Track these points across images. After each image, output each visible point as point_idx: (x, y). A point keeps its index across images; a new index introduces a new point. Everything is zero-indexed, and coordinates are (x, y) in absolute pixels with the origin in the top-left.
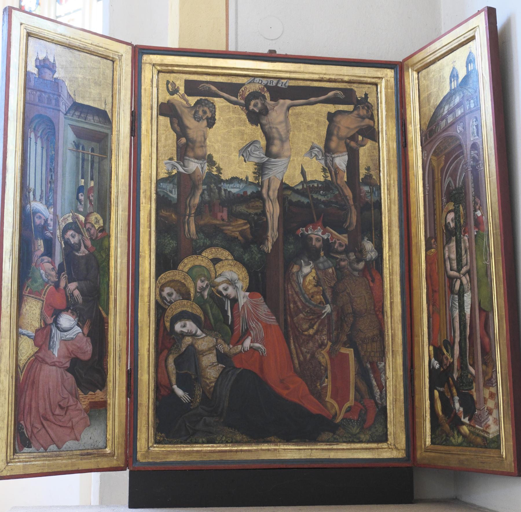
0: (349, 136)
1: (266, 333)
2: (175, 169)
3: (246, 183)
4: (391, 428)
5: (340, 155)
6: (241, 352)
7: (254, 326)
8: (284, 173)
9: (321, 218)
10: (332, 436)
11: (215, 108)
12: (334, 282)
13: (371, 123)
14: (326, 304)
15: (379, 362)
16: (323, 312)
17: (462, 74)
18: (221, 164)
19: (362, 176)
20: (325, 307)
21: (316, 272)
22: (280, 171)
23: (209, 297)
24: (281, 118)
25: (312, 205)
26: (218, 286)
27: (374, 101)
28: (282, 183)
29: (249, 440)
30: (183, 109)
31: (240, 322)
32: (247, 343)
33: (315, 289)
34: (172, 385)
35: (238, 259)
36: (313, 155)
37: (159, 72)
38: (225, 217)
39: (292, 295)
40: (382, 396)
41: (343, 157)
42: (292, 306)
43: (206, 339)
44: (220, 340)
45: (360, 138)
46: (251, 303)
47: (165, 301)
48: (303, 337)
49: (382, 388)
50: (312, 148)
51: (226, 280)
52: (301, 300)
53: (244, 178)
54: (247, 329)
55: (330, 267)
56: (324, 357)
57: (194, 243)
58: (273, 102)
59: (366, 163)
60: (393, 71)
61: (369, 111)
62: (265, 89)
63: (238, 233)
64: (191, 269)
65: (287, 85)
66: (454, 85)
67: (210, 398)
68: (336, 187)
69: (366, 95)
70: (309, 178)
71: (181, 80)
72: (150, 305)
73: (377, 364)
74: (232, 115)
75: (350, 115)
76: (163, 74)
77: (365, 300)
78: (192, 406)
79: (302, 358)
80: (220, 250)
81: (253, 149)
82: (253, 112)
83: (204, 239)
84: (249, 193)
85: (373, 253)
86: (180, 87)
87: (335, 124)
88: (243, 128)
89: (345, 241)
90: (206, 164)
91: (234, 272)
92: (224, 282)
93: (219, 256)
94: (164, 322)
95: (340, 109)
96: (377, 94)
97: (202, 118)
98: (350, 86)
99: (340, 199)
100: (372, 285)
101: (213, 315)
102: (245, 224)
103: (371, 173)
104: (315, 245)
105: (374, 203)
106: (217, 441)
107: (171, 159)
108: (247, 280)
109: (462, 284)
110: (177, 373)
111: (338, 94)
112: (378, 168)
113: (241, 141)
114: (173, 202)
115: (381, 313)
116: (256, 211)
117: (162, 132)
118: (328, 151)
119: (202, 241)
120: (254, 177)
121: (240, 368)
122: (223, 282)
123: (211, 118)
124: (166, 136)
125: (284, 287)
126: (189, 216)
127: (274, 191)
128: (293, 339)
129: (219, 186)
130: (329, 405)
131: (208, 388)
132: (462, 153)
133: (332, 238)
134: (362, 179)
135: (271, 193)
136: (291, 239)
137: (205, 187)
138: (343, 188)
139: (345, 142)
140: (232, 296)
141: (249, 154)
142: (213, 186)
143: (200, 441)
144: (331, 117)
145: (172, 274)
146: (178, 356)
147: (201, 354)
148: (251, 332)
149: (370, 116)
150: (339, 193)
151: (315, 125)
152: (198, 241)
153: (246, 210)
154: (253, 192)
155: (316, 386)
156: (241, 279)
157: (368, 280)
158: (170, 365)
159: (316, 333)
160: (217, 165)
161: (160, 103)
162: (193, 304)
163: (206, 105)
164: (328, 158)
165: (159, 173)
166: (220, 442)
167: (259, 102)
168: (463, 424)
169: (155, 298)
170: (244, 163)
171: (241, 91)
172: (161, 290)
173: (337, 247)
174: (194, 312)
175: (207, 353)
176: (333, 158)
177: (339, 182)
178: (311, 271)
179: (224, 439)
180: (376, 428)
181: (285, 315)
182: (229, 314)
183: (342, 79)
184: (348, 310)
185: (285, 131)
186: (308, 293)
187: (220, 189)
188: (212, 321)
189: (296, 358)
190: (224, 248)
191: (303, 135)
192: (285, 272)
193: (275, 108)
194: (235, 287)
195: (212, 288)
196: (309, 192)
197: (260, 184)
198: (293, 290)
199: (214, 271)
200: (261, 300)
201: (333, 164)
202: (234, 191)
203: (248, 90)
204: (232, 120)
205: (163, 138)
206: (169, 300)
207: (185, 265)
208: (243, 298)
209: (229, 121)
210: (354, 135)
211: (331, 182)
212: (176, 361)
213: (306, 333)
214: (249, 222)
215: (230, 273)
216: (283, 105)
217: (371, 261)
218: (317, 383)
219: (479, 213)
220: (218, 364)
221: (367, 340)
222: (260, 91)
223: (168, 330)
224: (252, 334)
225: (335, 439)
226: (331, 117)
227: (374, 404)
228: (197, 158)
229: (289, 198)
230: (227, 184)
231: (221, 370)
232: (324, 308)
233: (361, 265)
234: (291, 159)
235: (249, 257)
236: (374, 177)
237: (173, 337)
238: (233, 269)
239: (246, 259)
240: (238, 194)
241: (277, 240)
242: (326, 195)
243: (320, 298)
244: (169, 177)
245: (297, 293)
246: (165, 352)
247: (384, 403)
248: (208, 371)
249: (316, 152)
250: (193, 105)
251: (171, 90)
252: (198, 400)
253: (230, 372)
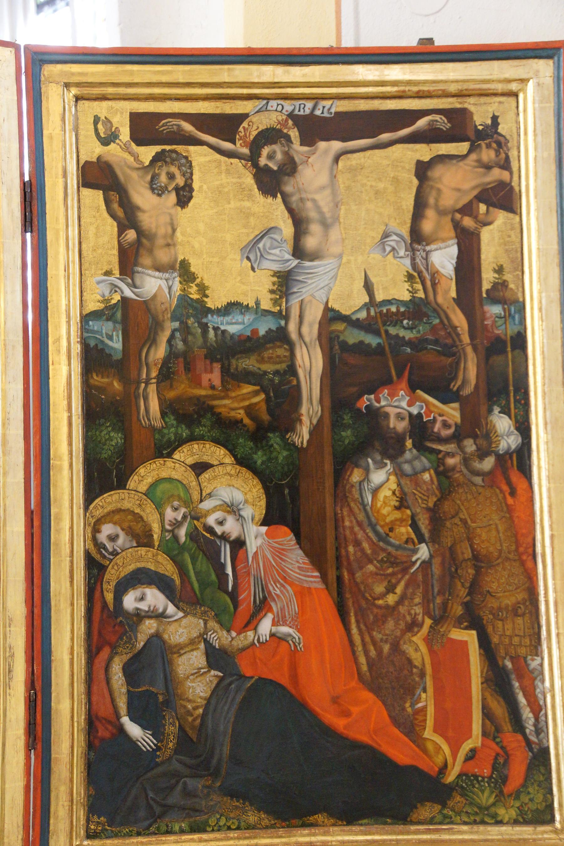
0: (460, 205)
1: (302, 605)
2: (116, 291)
3: (256, 313)
5: (442, 245)
6: (253, 644)
7: (278, 592)
8: (331, 289)
9: (406, 374)
10: (440, 812)
11: (191, 167)
12: (435, 499)
13: (505, 175)
14: (420, 543)
15: (529, 657)
16: (414, 559)
18: (205, 277)
19: (486, 286)
20: (418, 549)
21: (399, 481)
22: (322, 285)
23: (188, 538)
24: (323, 178)
25: (387, 348)
26: (206, 516)
27: (511, 131)
28: (327, 309)
29: (273, 822)
30: (128, 171)
31: (249, 585)
33: (397, 515)
34: (118, 717)
36: (388, 249)
37: (78, 99)
38: (217, 382)
39: (351, 528)
40: (540, 726)
41: (448, 250)
42: (351, 549)
43: (184, 621)
44: (212, 624)
45: (483, 208)
46: (272, 547)
47: (104, 552)
48: (375, 610)
50: (386, 235)
51: (220, 505)
52: (369, 537)
53: (252, 304)
54: (265, 598)
55: (424, 470)
57: (157, 436)
58: (306, 149)
59: (496, 258)
60: (551, 62)
61: (500, 153)
62: (290, 122)
63: (242, 412)
64: (153, 486)
65: (333, 110)
67: (195, 740)
68: (435, 310)
69: (495, 119)
70: (380, 297)
71: (122, 113)
72: (72, 562)
73: (526, 661)
74: (224, 179)
75: (461, 164)
76: (87, 103)
77: (498, 532)
78: (159, 756)
79: (373, 653)
80: (208, 446)
81: (268, 245)
82: (267, 169)
83: (177, 427)
84: (262, 332)
85: (512, 438)
86: (121, 129)
87: (431, 183)
88: (247, 204)
89: (454, 416)
90: (178, 279)
91: (237, 488)
92: (218, 508)
93: (206, 459)
94: (102, 592)
95: (440, 153)
96: (518, 114)
97: (166, 188)
98: (460, 103)
99: (442, 333)
100: (510, 501)
101: (197, 574)
102: (256, 393)
103: (505, 278)
104: (394, 428)
105: (512, 337)
106: (210, 826)
107: (108, 273)
108: (263, 503)
110: (128, 691)
111: (437, 121)
112: (520, 267)
113: (244, 231)
114: (115, 358)
115: (530, 557)
116: (278, 367)
117: (88, 220)
119: (173, 430)
120: (271, 299)
121: (252, 677)
122: (215, 509)
123: (183, 188)
124: (97, 228)
125: (336, 514)
126: (147, 383)
127: (311, 325)
128: (356, 615)
129: (204, 320)
130: (430, 747)
131: (190, 719)
133: (429, 412)
134: (488, 291)
135: (305, 330)
136: (347, 419)
137: (176, 324)
138: (449, 312)
139: (453, 220)
140: (233, 537)
141: (262, 255)
142: (191, 321)
143: (177, 828)
145: (116, 497)
146: (131, 659)
147: (175, 653)
148: (273, 604)
149: (502, 162)
150: (442, 321)
151: (391, 189)
152: (166, 431)
153: (257, 365)
154: (270, 329)
155: (404, 709)
156: (250, 500)
157: (501, 491)
158: (116, 677)
159: (400, 602)
160: (198, 281)
161: (82, 163)
162: (157, 555)
163: (172, 163)
164: (418, 253)
165: (86, 301)
166: (215, 828)
167: (278, 150)
169: (85, 546)
170: (251, 272)
171: (241, 129)
172: (96, 530)
173: (439, 429)
174: (161, 570)
175: (187, 649)
176: (428, 253)
177: (440, 300)
178: (388, 480)
179: (222, 822)
180: (529, 793)
181: (337, 568)
182: (229, 571)
183: (444, 91)
184: (463, 553)
185: (331, 205)
186: (382, 523)
187: (204, 327)
188: (196, 585)
189: (362, 653)
190: (217, 441)
191: (367, 210)
192: (336, 484)
193: (310, 160)
194: (240, 518)
195: (195, 522)
196: (381, 325)
197: (284, 313)
198: (353, 519)
199: (198, 488)
200: (290, 540)
201: (427, 265)
202: (233, 329)
203: (255, 127)
204: (226, 190)
205: (90, 232)
206: (111, 550)
207: (140, 478)
209: (220, 192)
210: (471, 202)
211: (425, 302)
212: (126, 669)
213: (380, 602)
214: (264, 390)
215: (228, 489)
216: (326, 152)
217: (509, 454)
218: (405, 702)
220: (209, 671)
221: (505, 613)
222: (279, 127)
223: (111, 607)
224: (275, 609)
225: (445, 817)
227: (523, 744)
228: (159, 268)
229: (342, 338)
230: (219, 316)
231: (215, 682)
232: (415, 551)
233: (488, 463)
234: (344, 260)
235: (264, 458)
236: (512, 286)
237: (121, 621)
238: (234, 482)
239: (259, 462)
240: (240, 336)
241: (320, 420)
242: (415, 328)
243: (408, 533)
244: (106, 307)
245: (360, 524)
246: (105, 653)
247: (545, 741)
248: (190, 684)
249: (393, 244)
250: (147, 163)
251: (103, 135)
252: (171, 745)
253: (233, 686)
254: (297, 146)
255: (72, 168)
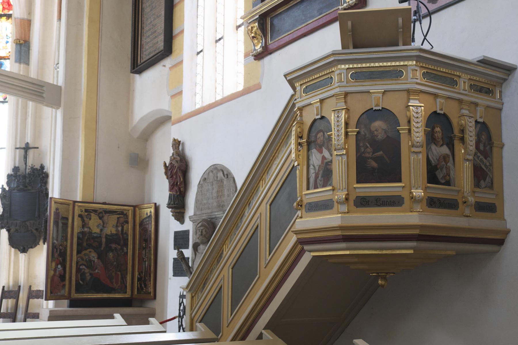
4: (128, 290)
17: (149, 214)
32: (97, 271)
35: (95, 251)
45: (124, 223)
49: (126, 281)
50: (113, 225)
56: (114, 274)
66: (147, 216)
70: (112, 233)
88: (97, 221)
107: (81, 228)
109: (146, 260)
118: (117, 226)
122: (91, 257)
132: (147, 232)
144: (118, 218)
168: (144, 289)
194: (94, 258)
208: (96, 260)
219: (150, 245)
226: (118, 218)
228: (87, 227)
233: (123, 253)
254: (104, 214)
255: (78, 215)
